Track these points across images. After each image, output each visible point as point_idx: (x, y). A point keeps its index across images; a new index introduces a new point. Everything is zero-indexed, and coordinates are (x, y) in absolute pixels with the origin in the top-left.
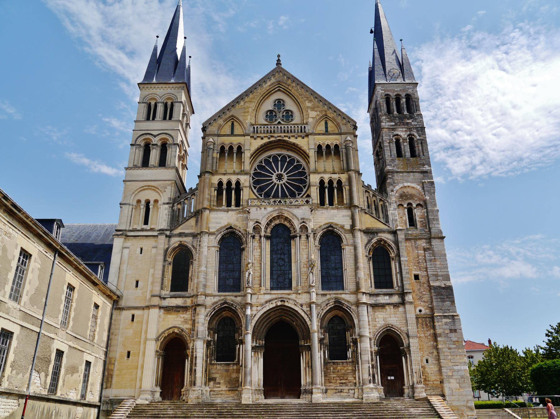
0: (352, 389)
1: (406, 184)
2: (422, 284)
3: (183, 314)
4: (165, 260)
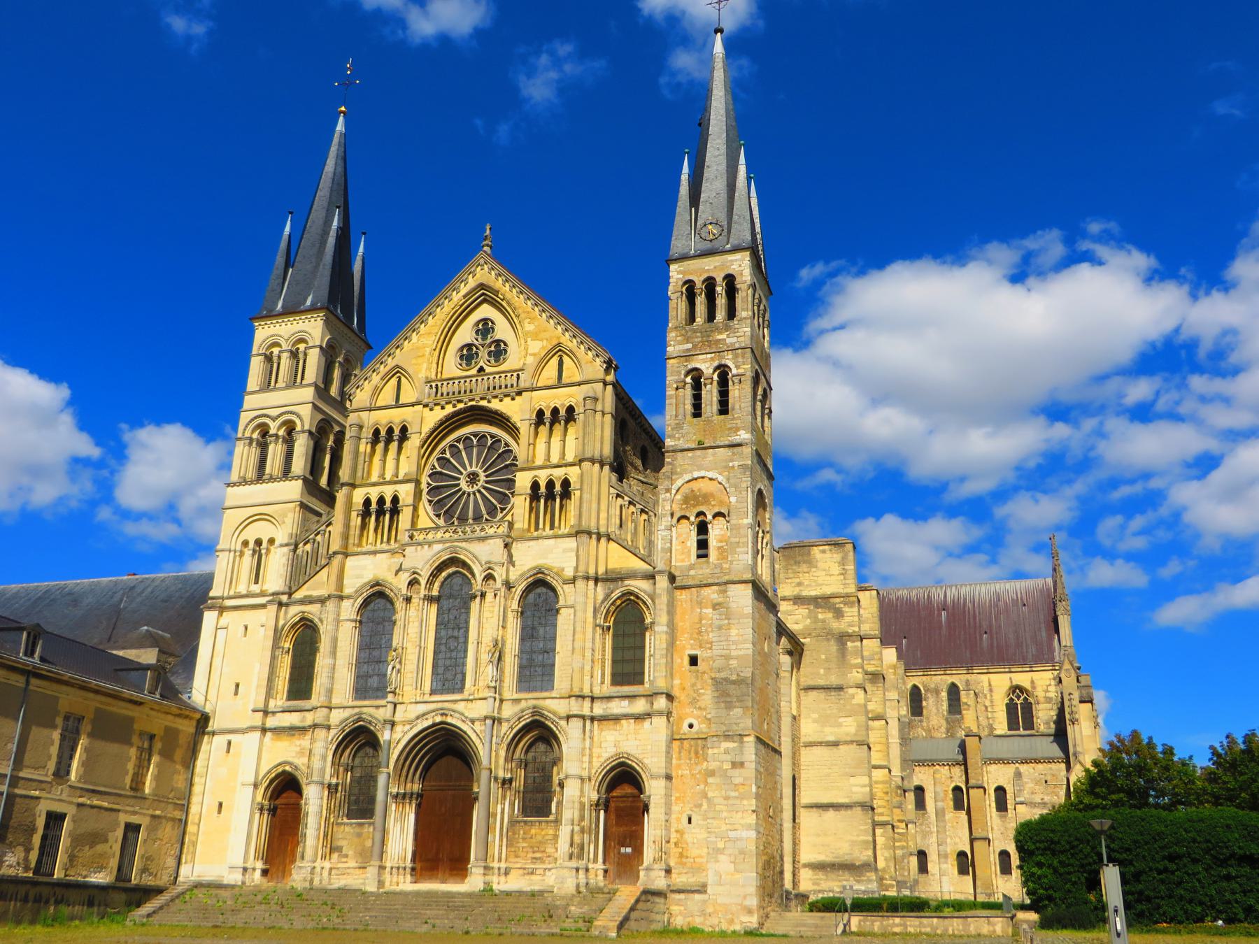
0: (550, 869)
1: (696, 474)
2: (699, 675)
3: (299, 739)
4: (276, 645)
